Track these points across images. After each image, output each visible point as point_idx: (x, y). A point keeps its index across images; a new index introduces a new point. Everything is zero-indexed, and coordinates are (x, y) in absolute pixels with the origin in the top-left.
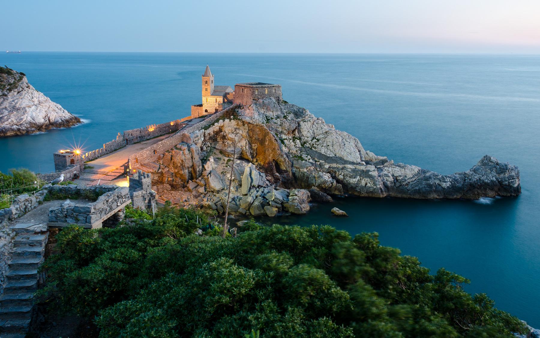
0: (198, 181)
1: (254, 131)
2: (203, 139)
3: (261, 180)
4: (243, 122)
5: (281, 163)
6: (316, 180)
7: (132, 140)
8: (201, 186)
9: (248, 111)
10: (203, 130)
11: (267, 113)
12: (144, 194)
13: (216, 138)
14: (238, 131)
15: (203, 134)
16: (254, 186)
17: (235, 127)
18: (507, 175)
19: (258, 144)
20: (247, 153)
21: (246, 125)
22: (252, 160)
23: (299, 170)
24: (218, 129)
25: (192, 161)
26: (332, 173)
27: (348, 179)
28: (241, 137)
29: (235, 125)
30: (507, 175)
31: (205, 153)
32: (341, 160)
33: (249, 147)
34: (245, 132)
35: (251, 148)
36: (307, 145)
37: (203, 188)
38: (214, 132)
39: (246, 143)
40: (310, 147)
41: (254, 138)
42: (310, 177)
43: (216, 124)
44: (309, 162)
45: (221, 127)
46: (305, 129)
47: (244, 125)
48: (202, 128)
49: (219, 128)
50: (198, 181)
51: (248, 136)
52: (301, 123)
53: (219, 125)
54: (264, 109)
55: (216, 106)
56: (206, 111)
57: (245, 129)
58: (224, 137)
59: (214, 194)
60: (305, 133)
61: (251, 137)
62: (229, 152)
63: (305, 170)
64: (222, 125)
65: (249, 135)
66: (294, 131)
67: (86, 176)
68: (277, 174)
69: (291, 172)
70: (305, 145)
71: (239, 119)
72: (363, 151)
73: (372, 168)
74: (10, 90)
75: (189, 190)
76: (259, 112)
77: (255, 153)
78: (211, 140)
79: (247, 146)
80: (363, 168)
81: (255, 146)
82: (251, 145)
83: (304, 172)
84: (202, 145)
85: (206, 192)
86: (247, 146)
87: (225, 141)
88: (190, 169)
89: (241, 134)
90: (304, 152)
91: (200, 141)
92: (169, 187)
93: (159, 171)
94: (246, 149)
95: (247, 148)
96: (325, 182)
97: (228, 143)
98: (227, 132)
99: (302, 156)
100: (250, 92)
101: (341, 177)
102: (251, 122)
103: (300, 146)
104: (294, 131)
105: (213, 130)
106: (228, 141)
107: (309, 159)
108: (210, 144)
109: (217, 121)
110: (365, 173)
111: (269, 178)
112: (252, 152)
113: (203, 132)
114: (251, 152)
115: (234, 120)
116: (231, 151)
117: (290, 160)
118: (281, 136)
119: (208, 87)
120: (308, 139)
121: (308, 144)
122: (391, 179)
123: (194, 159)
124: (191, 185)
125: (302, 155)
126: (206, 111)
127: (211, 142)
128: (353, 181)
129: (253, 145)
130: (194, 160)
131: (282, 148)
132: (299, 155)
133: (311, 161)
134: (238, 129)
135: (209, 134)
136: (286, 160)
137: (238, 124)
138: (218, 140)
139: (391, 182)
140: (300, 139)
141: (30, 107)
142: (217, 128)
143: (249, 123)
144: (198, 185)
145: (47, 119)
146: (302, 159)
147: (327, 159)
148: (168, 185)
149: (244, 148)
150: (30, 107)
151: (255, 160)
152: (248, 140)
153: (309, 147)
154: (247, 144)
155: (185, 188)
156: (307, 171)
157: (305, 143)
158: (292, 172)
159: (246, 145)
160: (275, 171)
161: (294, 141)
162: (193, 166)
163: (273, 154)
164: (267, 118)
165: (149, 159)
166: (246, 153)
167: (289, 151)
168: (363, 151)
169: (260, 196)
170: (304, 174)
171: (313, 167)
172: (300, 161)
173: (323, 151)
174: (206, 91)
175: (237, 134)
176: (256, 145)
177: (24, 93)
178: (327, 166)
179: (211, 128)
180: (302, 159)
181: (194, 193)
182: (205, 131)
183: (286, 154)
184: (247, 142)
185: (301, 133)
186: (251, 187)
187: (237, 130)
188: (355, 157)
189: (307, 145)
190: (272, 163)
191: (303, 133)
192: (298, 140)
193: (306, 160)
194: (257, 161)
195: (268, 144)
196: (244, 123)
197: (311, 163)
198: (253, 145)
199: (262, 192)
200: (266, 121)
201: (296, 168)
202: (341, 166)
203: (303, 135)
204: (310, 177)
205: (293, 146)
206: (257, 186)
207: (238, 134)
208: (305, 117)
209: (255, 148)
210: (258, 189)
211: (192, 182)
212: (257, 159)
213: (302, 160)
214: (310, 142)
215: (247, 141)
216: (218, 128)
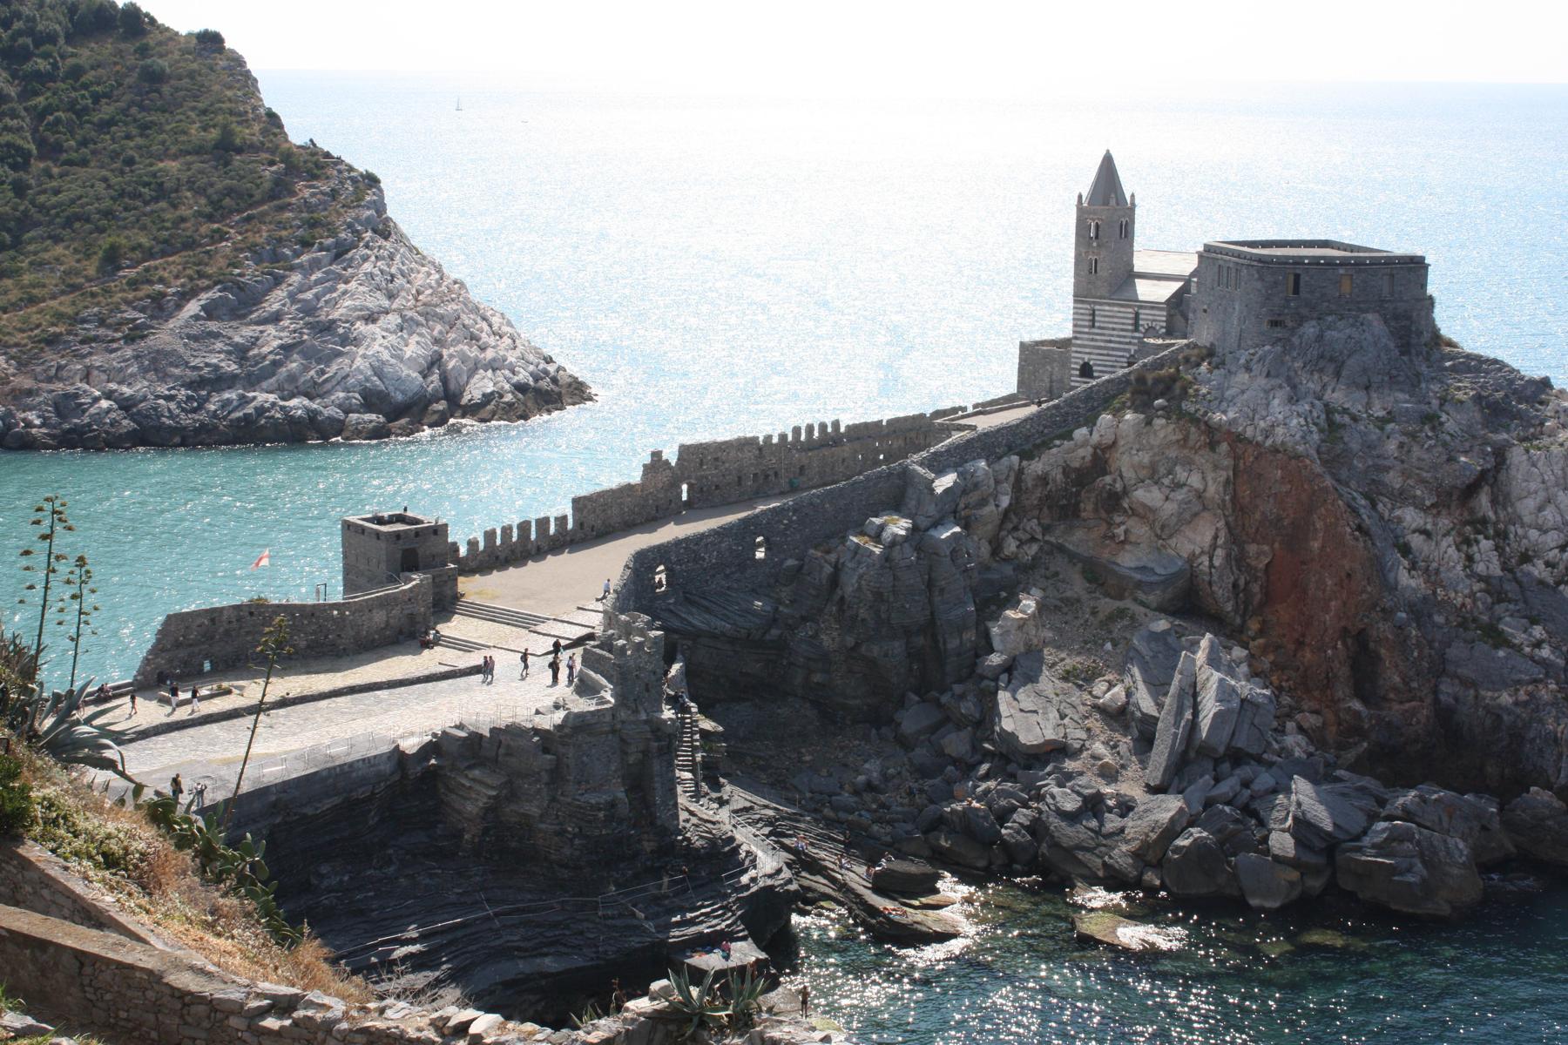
0: (944, 699)
1: (1259, 476)
2: (1005, 501)
3: (1246, 726)
5: (1383, 651)
6: (1560, 755)
7: (717, 487)
8: (959, 727)
9: (1243, 377)
10: (1015, 459)
11: (1335, 395)
12: (623, 722)
13: (1077, 504)
14: (1181, 473)
15: (1012, 479)
16: (1205, 751)
17: (1173, 453)
19: (1277, 545)
20: (1215, 588)
21: (1224, 447)
22: (1238, 621)
23: (1476, 697)
24: (1089, 458)
25: (930, 602)
28: (1197, 508)
29: (1170, 445)
31: (1008, 570)
33: (1228, 555)
34: (1214, 480)
35: (1238, 560)
36: (1538, 570)
37: (966, 734)
38: (1066, 470)
39: (1216, 537)
40: (1551, 581)
41: (1258, 516)
42: (1531, 735)
43: (1081, 433)
44: (1532, 658)
45: (1104, 451)
46: (1533, 486)
47: (1213, 445)
48: (1010, 449)
49: (1095, 455)
50: (944, 699)
51: (1229, 505)
52: (1517, 455)
53: (1096, 437)
54: (1321, 371)
55: (1133, 348)
56: (1086, 371)
57: (1216, 467)
58: (1113, 501)
59: (1011, 768)
60: (1527, 507)
61: (1242, 509)
62: (1127, 572)
63: (1506, 698)
64: (1108, 440)
65: (1234, 499)
66: (1471, 490)
67: (455, 627)
68: (1357, 705)
69: (1429, 700)
70: (1526, 567)
71: (1194, 420)
74: (306, 244)
75: (905, 743)
76: (1294, 387)
77: (1255, 588)
78: (1049, 508)
79: (1220, 552)
81: (1259, 554)
82: (1242, 551)
83: (1500, 707)
84: (1003, 533)
85: (978, 757)
86: (1220, 552)
87: (1118, 519)
88: (920, 641)
89: (1196, 490)
90: (1511, 607)
91: (990, 509)
93: (768, 637)
94: (1211, 566)
95: (1217, 563)
97: (1126, 532)
98: (1129, 474)
99: (1501, 626)
100: (1259, 285)
102: (1249, 433)
103: (1498, 572)
104: (1471, 490)
105: (1061, 462)
106: (1131, 522)
107: (1538, 644)
108: (1039, 529)
109: (1091, 422)
111: (1312, 720)
112: (1242, 582)
113: (1011, 468)
114: (1235, 585)
115: (1168, 418)
116: (1137, 569)
117: (1430, 643)
118: (1398, 513)
119: (1104, 253)
120: (1543, 538)
121: (1540, 563)
123: (942, 590)
124: (911, 720)
125: (1500, 619)
126: (1086, 371)
127: (1046, 521)
129: (1252, 549)
130: (937, 599)
131: (1391, 576)
132: (1485, 618)
133: (1545, 652)
134: (1188, 464)
135: (1043, 479)
136: (1408, 637)
137: (1186, 439)
138: (1083, 514)
140: (1501, 535)
141: (371, 318)
142: (1081, 452)
143: (1237, 439)
144: (947, 719)
146: (1500, 640)
148: (808, 705)
149: (1205, 560)
150: (374, 321)
151: (1254, 626)
152: (1227, 524)
153: (1541, 583)
154: (1220, 541)
155: (884, 730)
156: (1516, 703)
157: (1526, 558)
158: (1436, 701)
159: (1214, 546)
160: (1341, 691)
162: (931, 627)
163: (1345, 604)
164: (1330, 422)
165: (727, 576)
166: (1210, 584)
167: (1434, 593)
169: (1228, 803)
170: (1499, 717)
171: (1553, 686)
172: (1483, 647)
174: (1093, 277)
175: (1178, 486)
176: (1266, 548)
179: (1054, 450)
181: (921, 754)
182: (1025, 463)
183: (1412, 608)
184: (1222, 534)
185: (1512, 505)
186: (1192, 754)
187: (1178, 469)
190: (1335, 647)
191: (1518, 504)
192: (1487, 538)
193: (1518, 649)
194: (1262, 632)
195: (1323, 547)
196: (1217, 436)
197: (1543, 663)
198: (1252, 549)
199: (1246, 784)
200: (1321, 431)
201: (1461, 682)
203: (1520, 517)
204: (1531, 735)
206: (1222, 750)
207: (1185, 489)
208: (1542, 424)
209: (1261, 566)
210: (1226, 766)
211: (924, 701)
212: (1264, 622)
213: (1496, 647)
214: (1553, 555)
215: (1221, 524)
216: (1087, 452)
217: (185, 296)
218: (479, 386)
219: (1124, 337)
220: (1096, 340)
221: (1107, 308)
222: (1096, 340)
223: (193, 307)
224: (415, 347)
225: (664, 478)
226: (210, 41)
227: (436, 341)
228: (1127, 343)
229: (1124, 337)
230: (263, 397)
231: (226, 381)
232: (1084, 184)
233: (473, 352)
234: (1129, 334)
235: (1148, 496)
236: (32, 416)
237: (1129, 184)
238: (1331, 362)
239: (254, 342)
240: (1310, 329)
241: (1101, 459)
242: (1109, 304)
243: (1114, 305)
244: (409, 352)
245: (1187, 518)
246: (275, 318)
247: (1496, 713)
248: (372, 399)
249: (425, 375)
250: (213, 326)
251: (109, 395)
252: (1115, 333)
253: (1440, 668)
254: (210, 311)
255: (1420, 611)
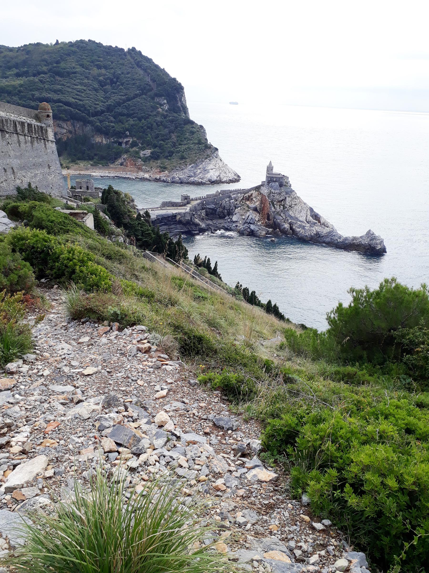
4: (261, 193)
18: (374, 242)
26: (290, 224)
27: (296, 228)
30: (374, 242)
32: (297, 219)
52: (287, 198)
58: (252, 199)
66: (282, 201)
72: (309, 216)
73: (308, 225)
74: (206, 158)
80: (304, 224)
92: (218, 216)
96: (285, 228)
101: (294, 227)
110: (304, 227)
122: (315, 232)
128: (298, 230)
139: (314, 234)
140: (284, 206)
145: (219, 178)
146: (280, 215)
147: (291, 217)
161: (280, 206)
168: (309, 216)
173: (290, 214)
177: (212, 160)
178: (290, 221)
180: (280, 215)
181: (226, 221)
188: (303, 219)
189: (286, 209)
202: (295, 222)
205: (278, 208)
217: (190, 165)
218: (224, 179)
223: (190, 166)
224: (217, 174)
225: (218, 193)
226: (201, 127)
227: (220, 173)
230: (196, 179)
231: (191, 176)
232: (268, 164)
233: (225, 175)
235: (254, 199)
236: (169, 179)
237: (273, 164)
238: (272, 187)
239: (197, 172)
240: (271, 184)
241: (252, 194)
244: (216, 174)
245: (257, 202)
246: (200, 168)
247: (278, 222)
248: (209, 180)
249: (217, 177)
250: (192, 169)
251: (178, 177)
253: (274, 218)
254: (192, 167)
255: (274, 212)
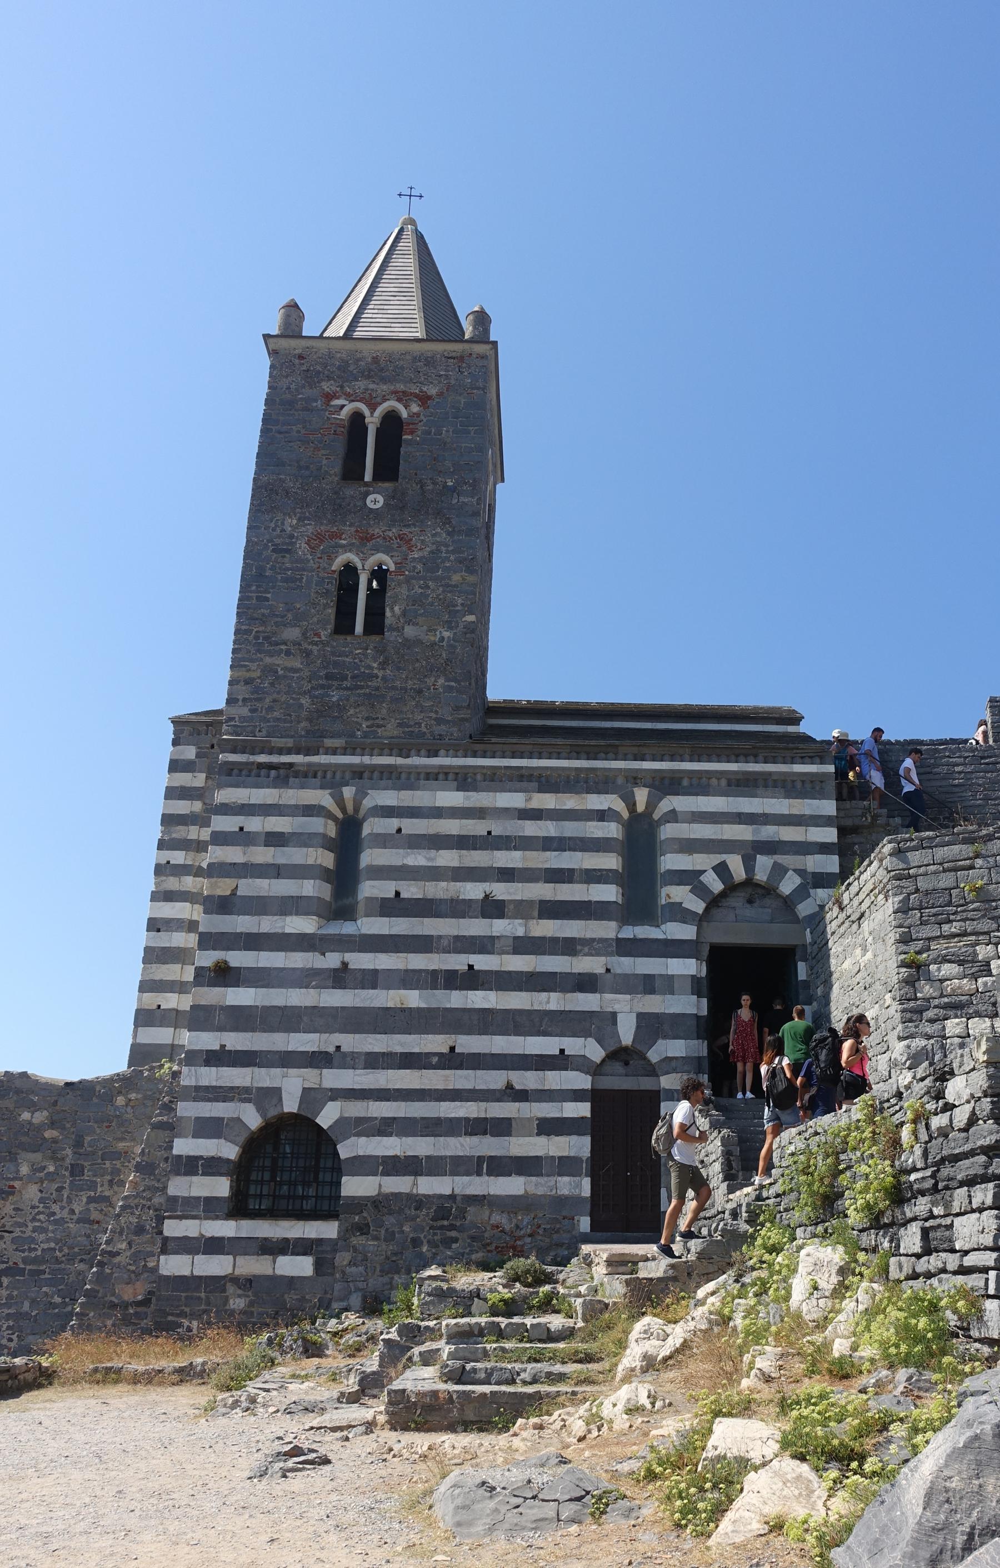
219: (569, 947)
220: (371, 979)
221: (450, 798)
222: (371, 979)
228: (586, 983)
229: (569, 947)
234: (606, 929)
242: (464, 780)
243: (495, 780)
252: (500, 927)
